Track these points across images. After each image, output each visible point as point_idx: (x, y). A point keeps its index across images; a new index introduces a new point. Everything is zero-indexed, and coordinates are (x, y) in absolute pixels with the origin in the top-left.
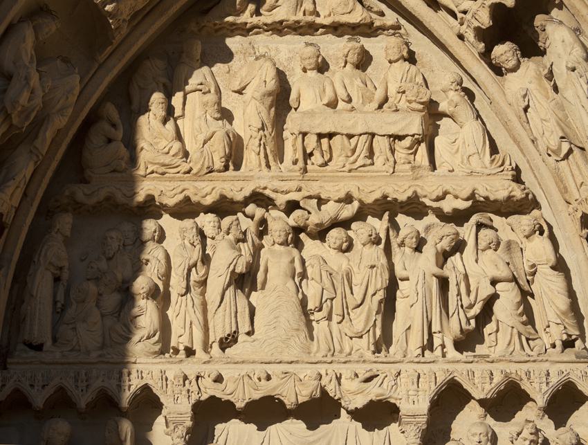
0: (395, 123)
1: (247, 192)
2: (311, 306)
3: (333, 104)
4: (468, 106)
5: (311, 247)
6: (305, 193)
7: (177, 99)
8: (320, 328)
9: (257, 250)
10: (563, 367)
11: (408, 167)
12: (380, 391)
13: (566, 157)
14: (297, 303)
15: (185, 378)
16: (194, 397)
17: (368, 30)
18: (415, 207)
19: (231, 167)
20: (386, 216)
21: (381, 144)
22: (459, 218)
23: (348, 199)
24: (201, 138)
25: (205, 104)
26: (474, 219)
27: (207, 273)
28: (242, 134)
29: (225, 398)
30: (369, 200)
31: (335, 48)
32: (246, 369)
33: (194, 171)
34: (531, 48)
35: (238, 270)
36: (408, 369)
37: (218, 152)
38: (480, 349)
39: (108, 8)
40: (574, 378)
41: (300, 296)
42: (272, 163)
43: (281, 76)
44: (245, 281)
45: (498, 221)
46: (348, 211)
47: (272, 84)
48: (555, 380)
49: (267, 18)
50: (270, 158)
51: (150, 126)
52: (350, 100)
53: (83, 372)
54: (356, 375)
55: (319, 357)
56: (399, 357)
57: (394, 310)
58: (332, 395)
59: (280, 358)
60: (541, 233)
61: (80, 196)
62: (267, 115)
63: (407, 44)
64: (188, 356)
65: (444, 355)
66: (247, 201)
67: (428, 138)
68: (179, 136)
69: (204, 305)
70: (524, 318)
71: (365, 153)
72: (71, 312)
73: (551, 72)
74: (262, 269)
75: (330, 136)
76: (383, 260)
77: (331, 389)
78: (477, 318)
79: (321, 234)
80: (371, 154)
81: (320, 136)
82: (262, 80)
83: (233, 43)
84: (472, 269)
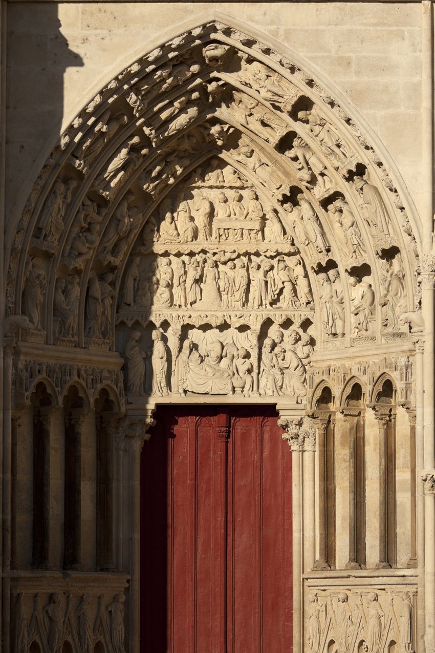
0: (251, 225)
1: (199, 250)
2: (221, 289)
3: (229, 216)
5: (222, 268)
6: (219, 250)
7: (175, 215)
8: (224, 297)
10: (306, 313)
11: (255, 240)
12: (244, 322)
13: (307, 245)
14: (217, 289)
15: (179, 316)
16: (182, 324)
17: (242, 188)
18: (257, 254)
19: (194, 240)
20: (247, 256)
21: (246, 232)
22: (272, 257)
23: (234, 252)
24: (184, 229)
25: (185, 217)
26: (278, 258)
27: (186, 278)
28: (198, 226)
29: (192, 324)
30: (241, 253)
31: (231, 194)
32: (199, 313)
33: (182, 242)
34: (296, 203)
35: (196, 278)
36: (254, 313)
38: (279, 304)
39: (152, 193)
40: (309, 317)
41: (218, 286)
42: (208, 238)
43: (211, 204)
44: (199, 281)
45: (286, 258)
46: (234, 256)
47: (208, 210)
48: (303, 318)
49: (207, 184)
50: (208, 236)
51: (165, 225)
52: (235, 215)
53: (144, 314)
54: (236, 316)
55: (224, 309)
56: (251, 309)
57: (249, 291)
58: (228, 322)
59: (210, 309)
60: (300, 264)
61: (143, 251)
62: (206, 221)
63: (256, 194)
64: (179, 307)
65: (266, 307)
66: (199, 253)
67: (262, 230)
68: (176, 229)
69: (185, 289)
70: (294, 294)
71: (240, 235)
72: (140, 292)
73: (302, 217)
74: (204, 276)
75: (228, 229)
76: (246, 274)
77: (228, 321)
78: (277, 294)
79: (225, 263)
80: (242, 234)
81: (225, 229)
82: (206, 208)
83: (195, 192)
84: (276, 277)
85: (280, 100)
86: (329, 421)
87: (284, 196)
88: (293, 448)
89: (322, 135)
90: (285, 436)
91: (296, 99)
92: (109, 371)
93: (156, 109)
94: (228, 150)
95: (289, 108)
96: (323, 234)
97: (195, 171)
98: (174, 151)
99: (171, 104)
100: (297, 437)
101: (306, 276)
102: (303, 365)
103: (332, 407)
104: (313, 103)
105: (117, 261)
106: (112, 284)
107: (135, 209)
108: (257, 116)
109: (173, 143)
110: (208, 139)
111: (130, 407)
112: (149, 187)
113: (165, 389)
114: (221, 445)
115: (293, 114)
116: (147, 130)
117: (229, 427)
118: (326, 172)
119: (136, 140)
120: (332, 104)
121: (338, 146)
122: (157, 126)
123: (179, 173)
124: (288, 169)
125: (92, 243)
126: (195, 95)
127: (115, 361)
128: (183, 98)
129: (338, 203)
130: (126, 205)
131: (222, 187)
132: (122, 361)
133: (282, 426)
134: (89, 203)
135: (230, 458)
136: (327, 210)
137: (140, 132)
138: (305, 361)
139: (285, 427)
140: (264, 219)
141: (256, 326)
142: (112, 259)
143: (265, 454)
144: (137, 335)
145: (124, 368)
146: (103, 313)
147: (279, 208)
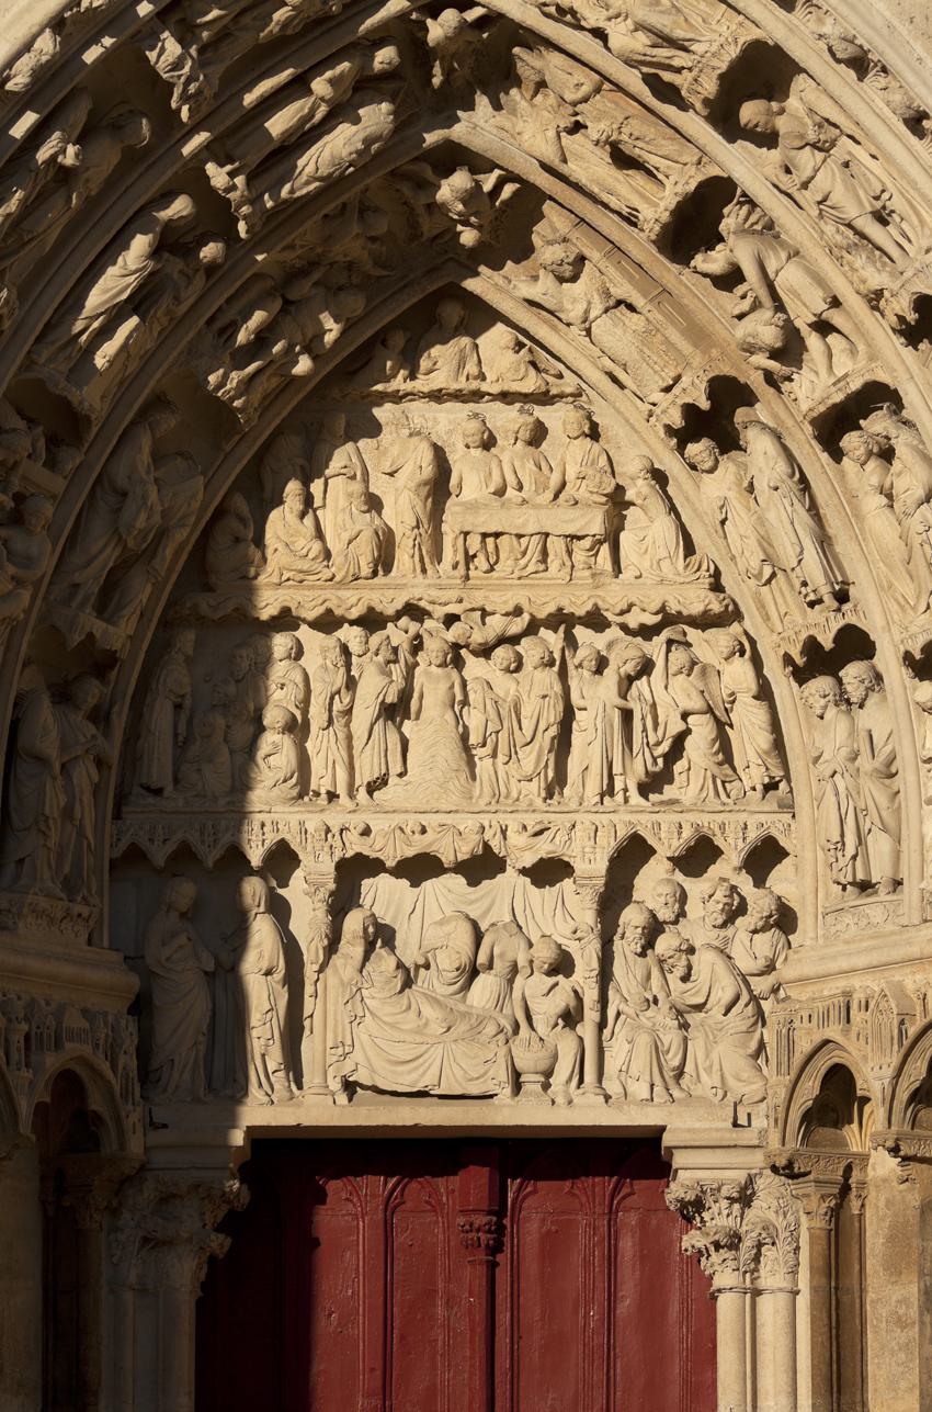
0: (573, 521)
1: (399, 605)
2: (473, 740)
3: (500, 492)
4: (660, 499)
5: (474, 667)
6: (466, 605)
7: (316, 487)
8: (484, 766)
9: (409, 676)
10: (763, 818)
11: (587, 573)
12: (551, 847)
13: (769, 582)
14: (457, 738)
15: (328, 830)
16: (338, 855)
17: (545, 398)
18: (596, 621)
19: (381, 573)
20: (562, 628)
21: (556, 546)
22: (647, 632)
23: (518, 611)
24: (346, 536)
25: (350, 495)
26: (666, 634)
27: (353, 700)
28: (393, 527)
29: (373, 855)
30: (542, 614)
31: (505, 419)
32: (397, 819)
33: (337, 579)
34: (729, 442)
35: (389, 700)
36: (585, 820)
37: (365, 553)
38: (669, 792)
39: (237, 403)
40: (775, 833)
41: (461, 729)
42: (428, 566)
43: (440, 455)
44: (396, 711)
45: (693, 635)
47: (428, 471)
48: (753, 835)
49: (422, 384)
50: (427, 560)
51: (282, 524)
52: (520, 488)
53: (210, 824)
54: (525, 827)
55: (482, 804)
56: (574, 806)
57: (569, 745)
58: (496, 851)
59: (436, 806)
60: (742, 653)
61: (204, 609)
62: (422, 509)
63: (589, 417)
64: (330, 801)
65: (626, 800)
66: (398, 615)
67: (612, 538)
69: (349, 738)
70: (720, 756)
71: (537, 556)
73: (751, 484)
74: (416, 695)
75: (497, 535)
76: (558, 688)
77: (496, 845)
78: (666, 756)
79: (485, 652)
80: (545, 553)
81: (485, 535)
82: (420, 463)
83: (383, 413)
84: (662, 697)
85: (680, 59)
86: (845, 1189)
87: (690, 410)
88: (717, 1282)
89: (822, 182)
90: (692, 1240)
91: (734, 52)
92: (85, 1012)
93: (249, 99)
94: (497, 266)
95: (710, 87)
96: (824, 541)
97: (381, 339)
98: (313, 264)
99: (299, 86)
100: (734, 1242)
101: (764, 693)
102: (755, 999)
103: (854, 1138)
104: (797, 69)
105: (116, 635)
106: (100, 717)
107: (180, 463)
108: (596, 129)
109: (307, 233)
110: (428, 227)
111: (157, 1137)
112: (226, 381)
113: (279, 1079)
114: (472, 1275)
115: (723, 116)
116: (217, 175)
117: (500, 1212)
118: (836, 318)
119: (180, 207)
120: (860, 64)
121: (882, 218)
122: (255, 159)
123: (329, 338)
124: (702, 317)
125: (28, 562)
126: (385, 56)
127: (108, 979)
128: (345, 65)
129: (878, 423)
130: (145, 442)
131: (477, 396)
132: (134, 981)
133: (683, 1204)
134: (21, 424)
135: (504, 1318)
136: (837, 455)
137: (194, 181)
138: (761, 985)
139: (692, 1210)
140: (618, 502)
141: (593, 864)
142: (98, 627)
143: (625, 1306)
144: (184, 892)
145: (141, 1007)
146: (68, 813)
147: (671, 463)
